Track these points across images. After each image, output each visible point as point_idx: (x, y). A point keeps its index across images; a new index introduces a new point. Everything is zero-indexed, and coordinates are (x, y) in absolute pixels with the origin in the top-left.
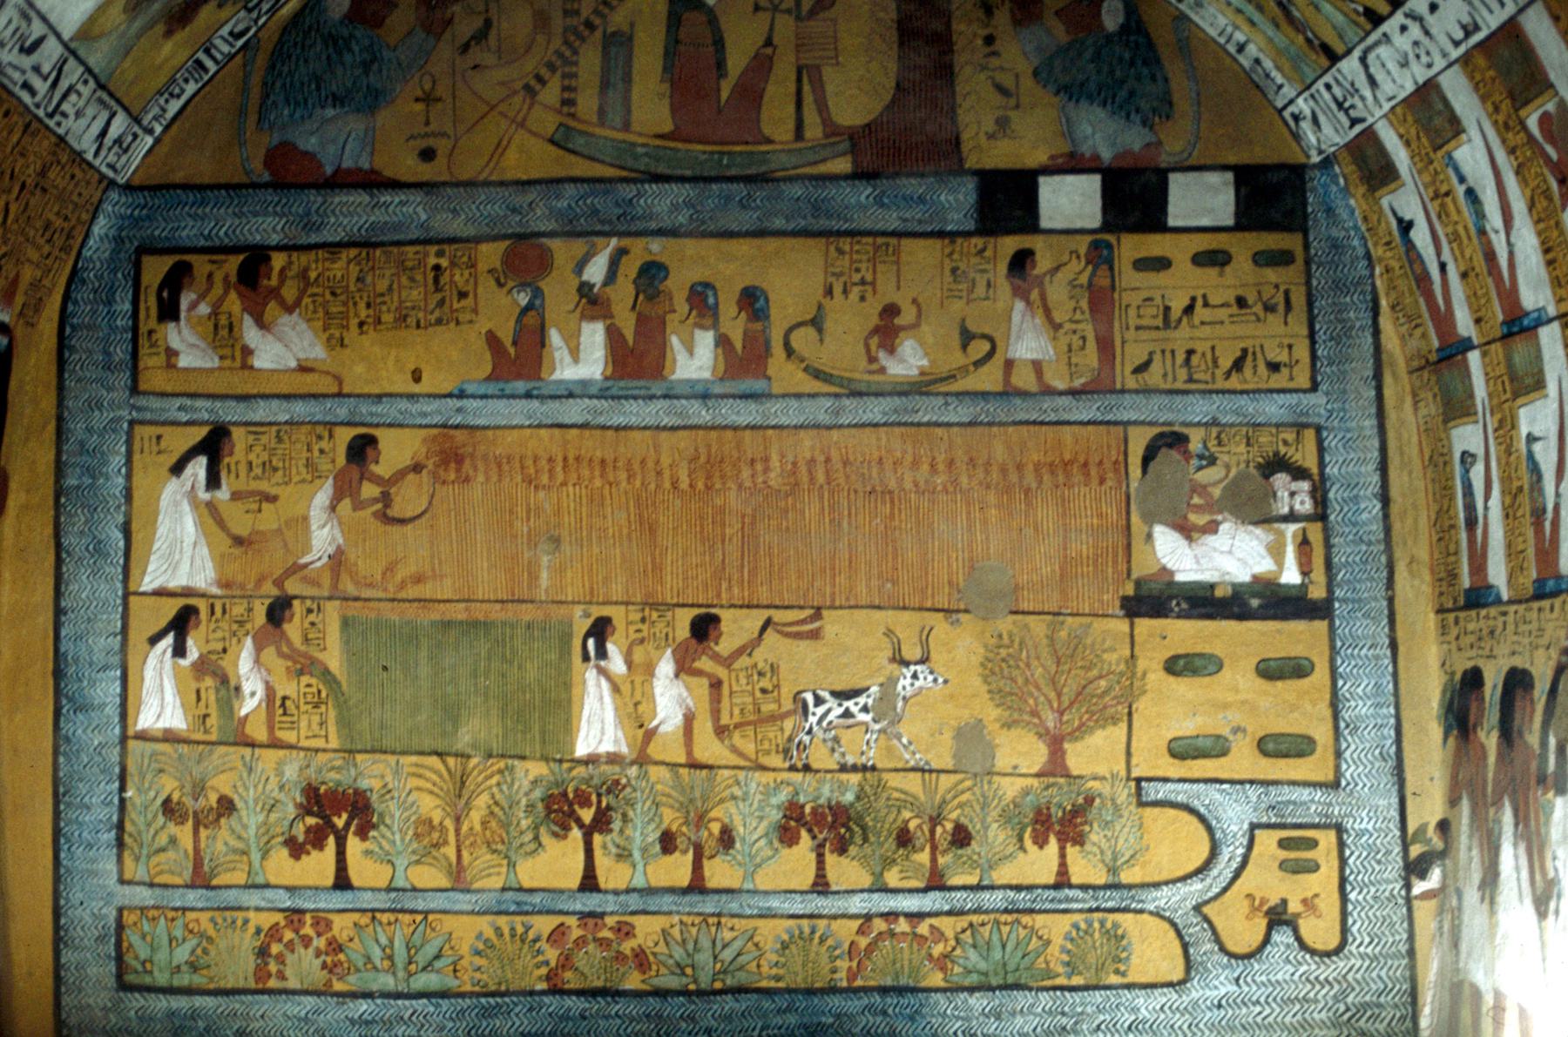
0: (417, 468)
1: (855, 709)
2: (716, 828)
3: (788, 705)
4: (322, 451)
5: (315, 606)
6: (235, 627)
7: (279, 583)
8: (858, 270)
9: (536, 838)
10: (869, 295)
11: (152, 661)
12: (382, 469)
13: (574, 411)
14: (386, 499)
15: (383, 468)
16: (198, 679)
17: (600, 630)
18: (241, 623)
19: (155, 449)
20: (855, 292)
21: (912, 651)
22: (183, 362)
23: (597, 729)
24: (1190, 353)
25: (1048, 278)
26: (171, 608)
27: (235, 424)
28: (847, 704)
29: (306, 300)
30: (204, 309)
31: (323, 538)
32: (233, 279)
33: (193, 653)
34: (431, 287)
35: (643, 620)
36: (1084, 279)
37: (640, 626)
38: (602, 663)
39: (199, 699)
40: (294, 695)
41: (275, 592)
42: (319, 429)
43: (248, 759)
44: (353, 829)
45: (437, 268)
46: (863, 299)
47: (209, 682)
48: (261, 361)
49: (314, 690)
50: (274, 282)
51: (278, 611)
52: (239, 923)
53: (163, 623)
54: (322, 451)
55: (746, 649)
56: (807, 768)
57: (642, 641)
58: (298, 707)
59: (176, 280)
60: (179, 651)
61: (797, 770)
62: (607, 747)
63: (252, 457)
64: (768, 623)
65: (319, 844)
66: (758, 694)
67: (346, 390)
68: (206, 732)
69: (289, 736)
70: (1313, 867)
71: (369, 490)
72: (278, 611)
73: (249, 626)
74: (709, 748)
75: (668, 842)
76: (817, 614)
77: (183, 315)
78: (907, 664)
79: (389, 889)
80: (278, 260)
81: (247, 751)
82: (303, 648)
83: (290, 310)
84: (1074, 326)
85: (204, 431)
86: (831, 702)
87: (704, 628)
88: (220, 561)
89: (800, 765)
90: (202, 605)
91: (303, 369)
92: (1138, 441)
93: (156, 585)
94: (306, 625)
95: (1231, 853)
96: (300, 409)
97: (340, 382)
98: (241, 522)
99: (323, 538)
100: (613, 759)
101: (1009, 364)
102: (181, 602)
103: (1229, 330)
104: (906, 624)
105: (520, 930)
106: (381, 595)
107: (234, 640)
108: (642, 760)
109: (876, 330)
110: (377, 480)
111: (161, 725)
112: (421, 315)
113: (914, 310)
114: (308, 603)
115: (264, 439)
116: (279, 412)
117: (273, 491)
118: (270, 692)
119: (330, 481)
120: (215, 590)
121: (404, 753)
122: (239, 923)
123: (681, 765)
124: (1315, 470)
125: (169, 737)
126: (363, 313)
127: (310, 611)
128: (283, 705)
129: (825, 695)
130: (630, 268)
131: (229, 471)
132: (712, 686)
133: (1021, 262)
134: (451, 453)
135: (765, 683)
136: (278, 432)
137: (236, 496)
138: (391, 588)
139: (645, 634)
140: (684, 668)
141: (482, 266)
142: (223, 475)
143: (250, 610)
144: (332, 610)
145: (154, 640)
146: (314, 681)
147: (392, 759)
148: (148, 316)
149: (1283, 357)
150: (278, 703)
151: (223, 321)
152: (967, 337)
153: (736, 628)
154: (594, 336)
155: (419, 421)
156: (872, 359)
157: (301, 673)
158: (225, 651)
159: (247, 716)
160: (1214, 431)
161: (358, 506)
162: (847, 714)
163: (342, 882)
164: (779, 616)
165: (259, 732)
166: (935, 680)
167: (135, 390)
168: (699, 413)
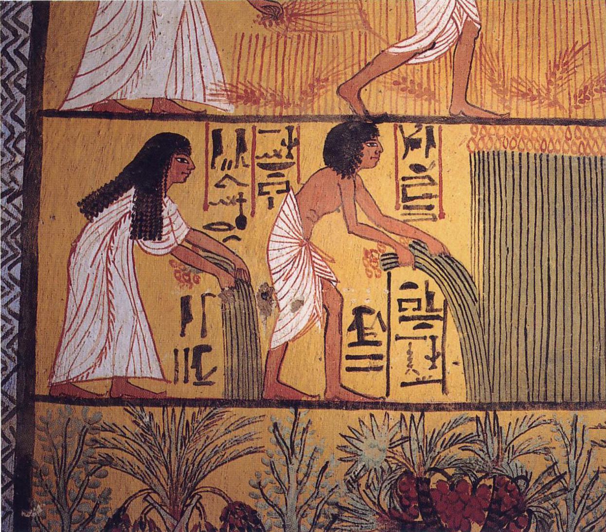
5: (422, 135)
6: (262, 175)
7: (350, 91)
40: (380, 306)
41: (343, 109)
51: (348, 146)
58: (386, 328)
60: (147, 225)
81: (284, 416)
107: (262, 201)
111: (105, 371)
120: (224, 107)
127: (412, 144)
128: (357, 325)
145: (93, 205)
150: (348, 318)
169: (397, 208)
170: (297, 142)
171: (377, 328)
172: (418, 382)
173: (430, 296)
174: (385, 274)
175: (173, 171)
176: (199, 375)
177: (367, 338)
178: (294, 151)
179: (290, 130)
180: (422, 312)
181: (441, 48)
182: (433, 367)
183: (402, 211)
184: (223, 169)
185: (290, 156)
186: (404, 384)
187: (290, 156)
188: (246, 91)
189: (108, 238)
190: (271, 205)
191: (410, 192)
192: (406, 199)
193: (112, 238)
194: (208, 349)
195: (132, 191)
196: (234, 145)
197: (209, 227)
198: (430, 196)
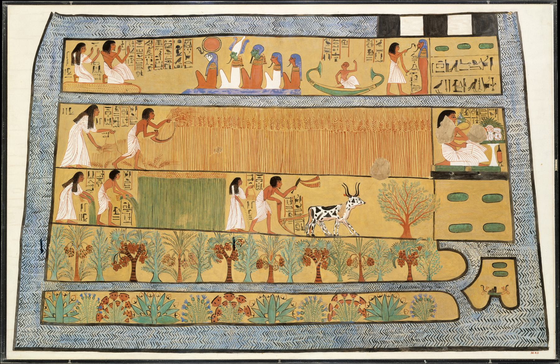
1: (331, 214)
2: (278, 259)
3: (306, 212)
4: (133, 114)
5: (128, 173)
8: (334, 50)
9: (210, 262)
10: (338, 59)
11: (64, 194)
13: (228, 100)
14: (156, 132)
15: (156, 121)
16: (82, 201)
17: (236, 182)
18: (100, 179)
19: (68, 113)
20: (333, 58)
21: (352, 192)
22: (81, 80)
23: (235, 219)
24: (456, 81)
25: (403, 54)
26: (71, 174)
27: (99, 104)
28: (328, 211)
29: (128, 58)
30: (89, 61)
31: (132, 146)
32: (101, 49)
33: (80, 190)
34: (175, 54)
35: (252, 179)
36: (417, 54)
37: (251, 181)
38: (237, 195)
39: (82, 208)
42: (132, 107)
44: (139, 258)
45: (178, 47)
46: (336, 60)
47: (86, 201)
48: (110, 81)
50: (116, 51)
51: (114, 174)
52: (92, 296)
55: (292, 190)
56: (313, 236)
57: (252, 187)
59: (79, 48)
60: (75, 189)
61: (309, 237)
62: (238, 227)
63: (106, 116)
64: (299, 180)
65: (125, 264)
66: (295, 208)
67: (142, 92)
69: (117, 223)
70: (505, 274)
72: (114, 174)
73: (102, 180)
74: (276, 228)
75: (259, 264)
76: (317, 178)
77: (81, 63)
78: (351, 196)
79: (151, 283)
80: (118, 43)
82: (123, 189)
83: (122, 62)
84: (413, 71)
86: (323, 211)
87: (275, 182)
88: (91, 156)
89: (311, 235)
90: (84, 172)
91: (127, 83)
92: (437, 112)
95: (474, 270)
96: (125, 99)
97: (140, 89)
98: (100, 140)
99: (132, 146)
100: (240, 231)
101: (389, 85)
103: (469, 72)
104: (351, 183)
105: (201, 298)
106: (154, 169)
108: (251, 232)
109: (340, 72)
110: (153, 125)
112: (171, 64)
113: (354, 64)
114: (126, 171)
116: (117, 99)
117: (113, 129)
118: (110, 205)
119: (136, 125)
122: (92, 296)
123: (265, 234)
124: (502, 124)
125: (70, 223)
126: (150, 63)
127: (126, 175)
128: (115, 210)
129: (320, 208)
130: (250, 48)
132: (278, 204)
133: (393, 48)
134: (181, 117)
135: (298, 203)
137: (99, 131)
138: (158, 166)
139: (253, 184)
140: (267, 196)
141: (195, 46)
144: (136, 175)
145: (65, 185)
146: (127, 201)
148: (67, 63)
149: (490, 82)
150: (113, 209)
151: (97, 66)
152: (374, 74)
153: (287, 182)
154: (236, 72)
156: (339, 83)
158: (93, 189)
160: (465, 110)
161: (146, 135)
162: (328, 215)
163: (133, 280)
164: (303, 178)
165: (104, 220)
166: (361, 202)
167: (61, 91)
168: (275, 101)
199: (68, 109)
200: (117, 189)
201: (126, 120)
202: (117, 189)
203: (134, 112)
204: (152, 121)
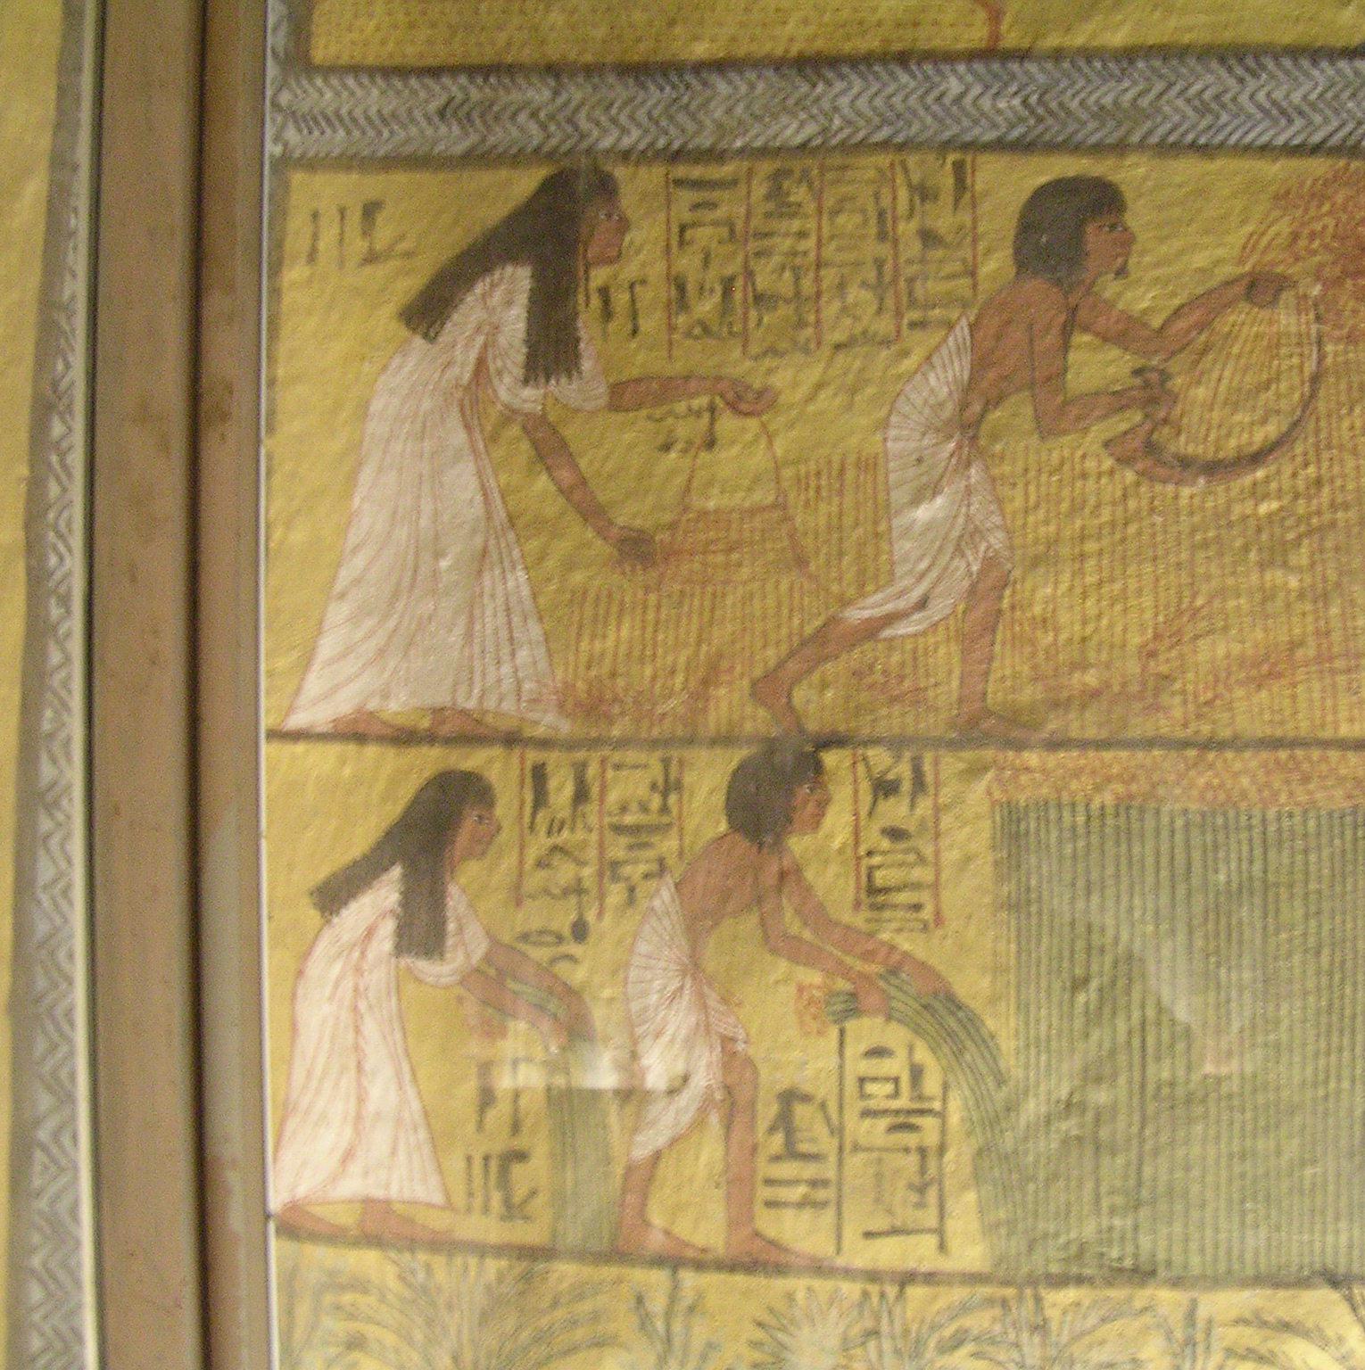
0: (1260, 287)
4: (928, 237)
5: (904, 770)
6: (618, 849)
7: (769, 688)
11: (326, 968)
12: (1142, 297)
19: (359, 246)
27: (625, 156)
40: (825, 1089)
41: (758, 720)
43: (657, 1304)
49: (895, 1065)
51: (772, 794)
53: (362, 838)
54: (928, 237)
58: (838, 1131)
60: (421, 931)
63: (687, 263)
68: (512, 1210)
71: (1095, 366)
81: (657, 1279)
82: (859, 920)
85: (526, 183)
93: (343, 705)
94: (872, 836)
102: (429, 761)
107: (616, 894)
110: (1125, 333)
111: (353, 1185)
114: (879, 757)
115: (730, 206)
120: (548, 721)
121: (1215, 1281)
125: (381, 1227)
127: (885, 788)
128: (784, 1122)
131: (607, 313)
136: (777, 177)
142: (587, 326)
143: (669, 786)
145: (333, 895)
146: (895, 1036)
147: (1168, 1300)
150: (768, 1111)
155: (1262, 133)
157: (852, 1007)
159: (657, 1156)
169: (857, 905)
170: (678, 786)
171: (821, 1130)
172: (894, 1231)
173: (917, 1073)
174: (834, 1032)
175: (463, 837)
176: (507, 1203)
177: (804, 1147)
178: (673, 798)
179: (666, 762)
180: (903, 1102)
181: (938, 609)
182: (921, 1205)
183: (865, 914)
184: (549, 833)
185: (664, 809)
186: (868, 1235)
187: (664, 809)
188: (589, 692)
189: (356, 954)
190: (631, 900)
191: (880, 878)
192: (873, 890)
193: (363, 953)
194: (521, 1156)
195: (396, 872)
196: (569, 790)
197: (525, 937)
198: (916, 886)
199: (355, 217)
200: (794, 925)
201: (879, 287)
202: (794, 925)
203: (944, 219)
204: (1110, 288)
